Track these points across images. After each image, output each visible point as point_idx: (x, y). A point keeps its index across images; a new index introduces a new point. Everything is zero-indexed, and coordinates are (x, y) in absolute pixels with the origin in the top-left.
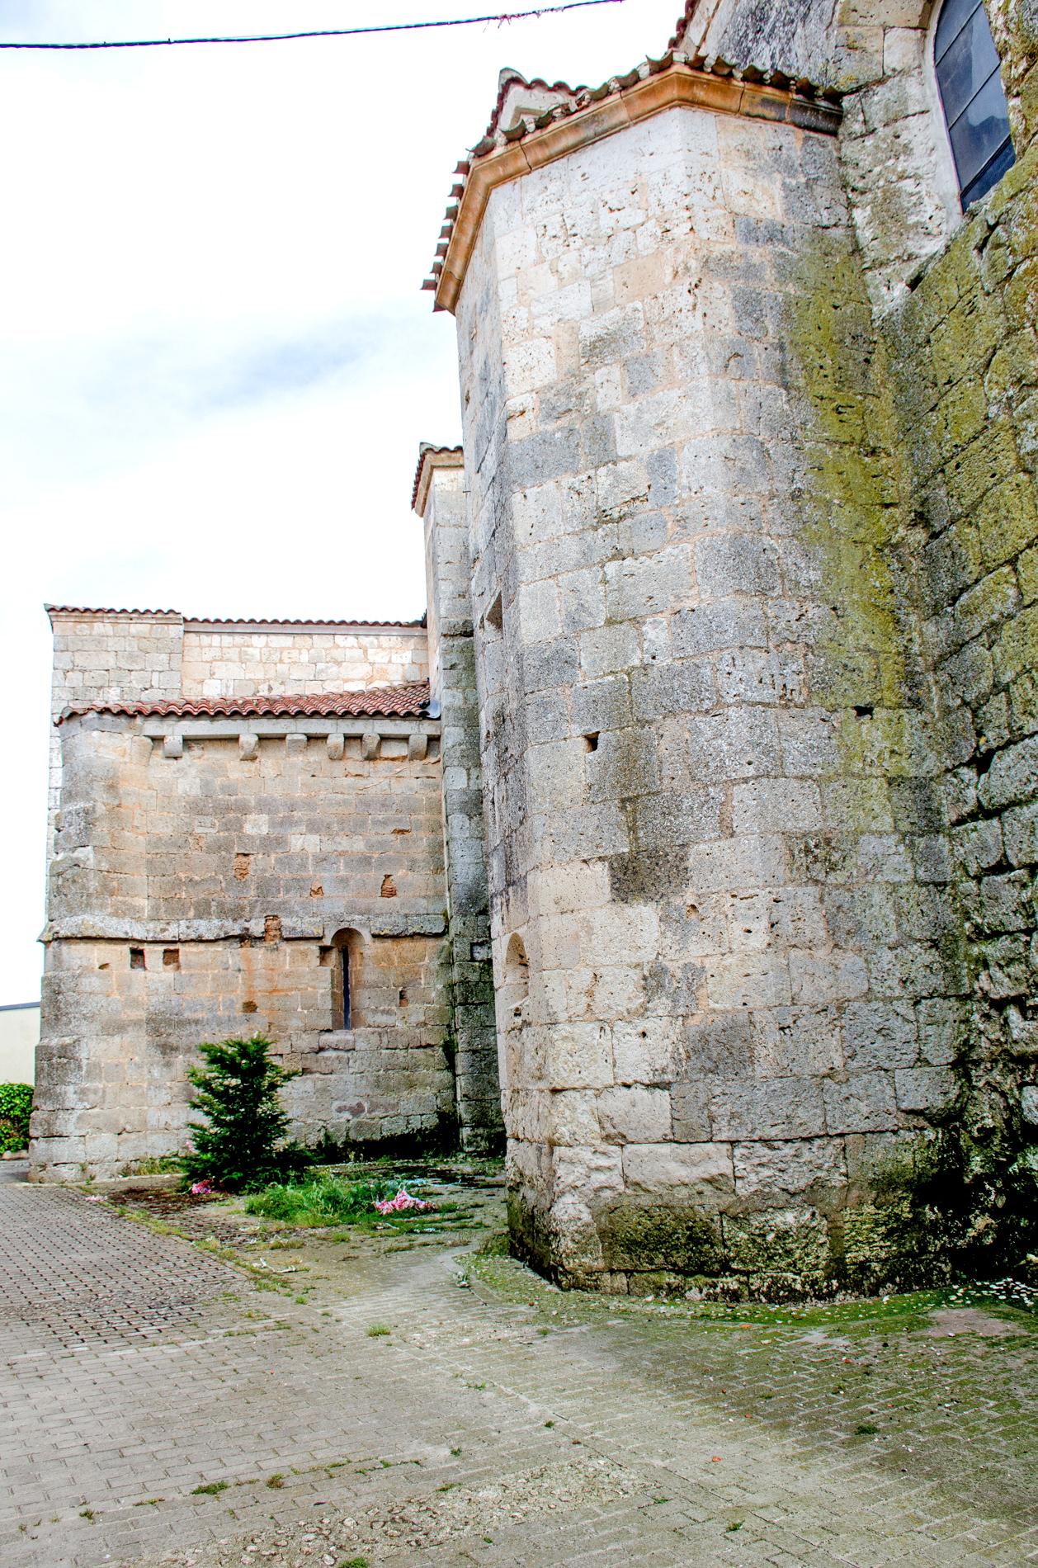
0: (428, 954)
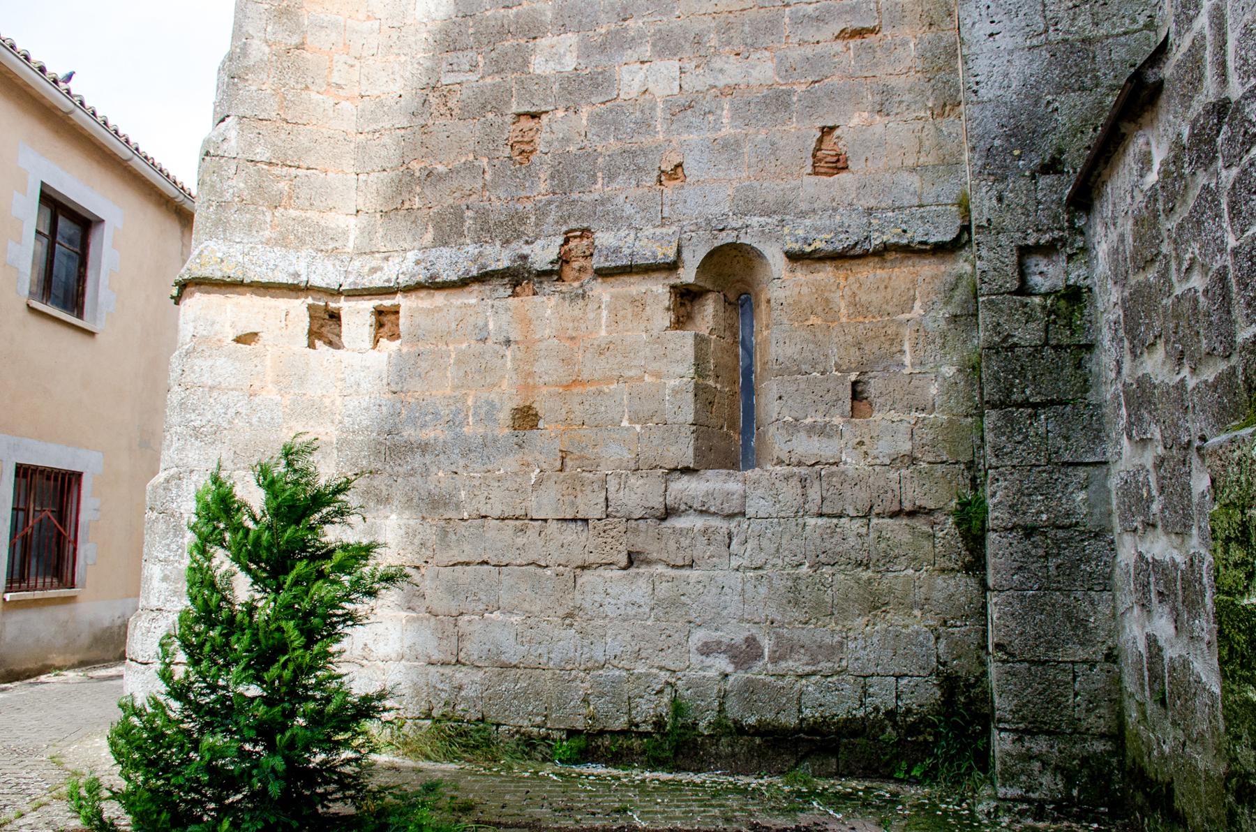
0: (919, 291)
